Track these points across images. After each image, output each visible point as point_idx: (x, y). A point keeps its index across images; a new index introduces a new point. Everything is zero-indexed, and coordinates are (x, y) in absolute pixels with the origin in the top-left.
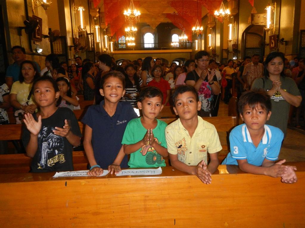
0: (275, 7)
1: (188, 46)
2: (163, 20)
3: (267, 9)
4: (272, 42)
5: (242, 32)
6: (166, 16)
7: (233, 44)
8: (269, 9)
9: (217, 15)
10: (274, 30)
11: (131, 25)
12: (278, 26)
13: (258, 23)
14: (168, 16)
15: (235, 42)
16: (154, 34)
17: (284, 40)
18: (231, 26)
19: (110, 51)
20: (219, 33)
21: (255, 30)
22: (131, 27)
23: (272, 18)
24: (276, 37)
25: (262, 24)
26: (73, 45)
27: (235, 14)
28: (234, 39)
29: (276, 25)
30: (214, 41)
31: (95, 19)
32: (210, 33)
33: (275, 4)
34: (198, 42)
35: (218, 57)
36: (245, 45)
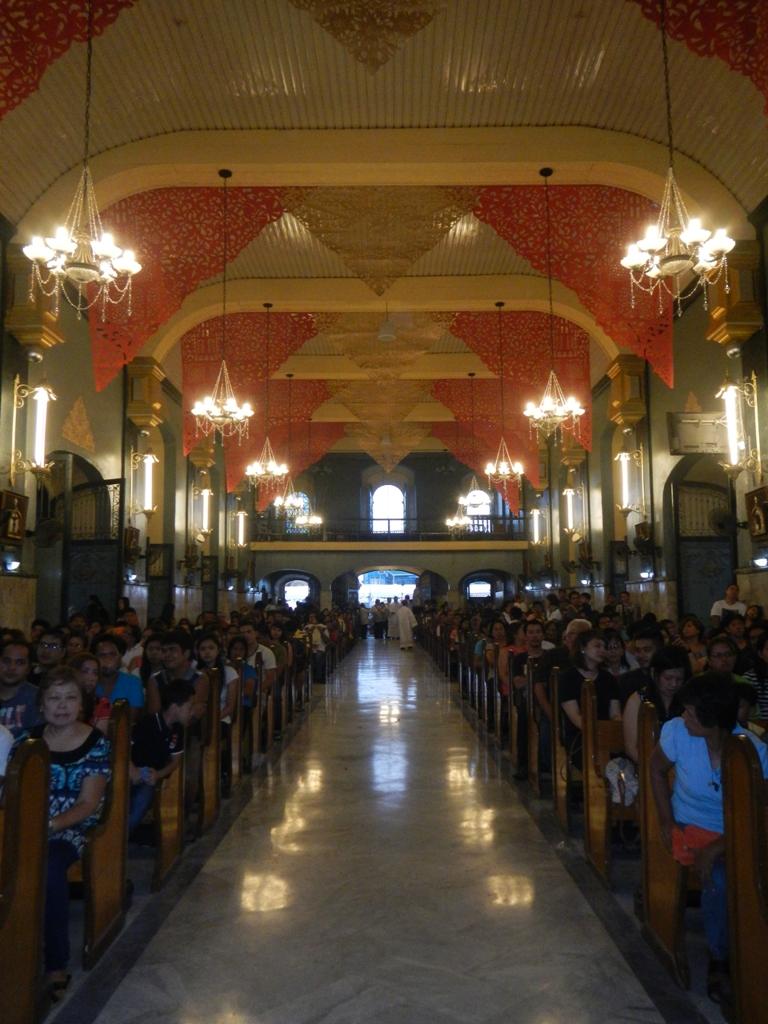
0: (755, 389)
1: (516, 530)
2: (419, 443)
4: (758, 517)
5: (665, 480)
6: (429, 430)
8: (730, 395)
9: (536, 417)
10: (760, 470)
11: (267, 453)
13: (698, 447)
14: (436, 429)
15: (646, 517)
16: (405, 488)
18: (623, 459)
19: (237, 541)
20: (597, 487)
21: (698, 476)
22: (268, 460)
23: (748, 430)
25: (710, 451)
27: (637, 418)
28: (641, 505)
30: (578, 514)
31: (146, 435)
32: (571, 488)
33: (754, 377)
35: (599, 569)
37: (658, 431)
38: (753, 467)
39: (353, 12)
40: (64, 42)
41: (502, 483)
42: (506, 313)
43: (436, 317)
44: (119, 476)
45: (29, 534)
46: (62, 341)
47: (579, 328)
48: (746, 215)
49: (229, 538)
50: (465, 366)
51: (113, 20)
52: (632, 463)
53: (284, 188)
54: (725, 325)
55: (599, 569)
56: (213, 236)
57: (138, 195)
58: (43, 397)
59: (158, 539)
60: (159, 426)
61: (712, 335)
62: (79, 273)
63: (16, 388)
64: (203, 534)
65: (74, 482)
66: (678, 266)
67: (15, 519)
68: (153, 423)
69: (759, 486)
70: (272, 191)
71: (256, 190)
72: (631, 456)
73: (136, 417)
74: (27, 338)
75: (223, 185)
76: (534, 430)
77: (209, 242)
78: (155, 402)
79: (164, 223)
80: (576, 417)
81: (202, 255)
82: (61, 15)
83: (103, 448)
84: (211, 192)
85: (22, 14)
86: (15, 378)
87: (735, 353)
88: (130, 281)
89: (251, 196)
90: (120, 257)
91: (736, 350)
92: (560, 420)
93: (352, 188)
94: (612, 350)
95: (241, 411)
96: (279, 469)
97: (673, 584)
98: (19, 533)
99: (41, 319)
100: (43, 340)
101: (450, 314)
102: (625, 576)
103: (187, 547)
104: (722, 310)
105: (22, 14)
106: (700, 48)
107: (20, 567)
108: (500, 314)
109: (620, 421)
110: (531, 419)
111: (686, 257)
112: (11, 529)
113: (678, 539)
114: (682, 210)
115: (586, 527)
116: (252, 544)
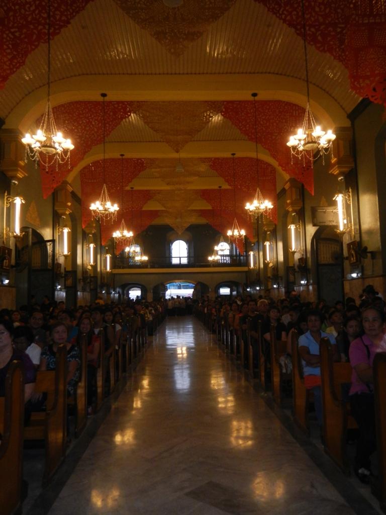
1: (242, 261)
2: (194, 220)
3: (337, 199)
5: (311, 238)
7: (299, 258)
8: (339, 199)
9: (251, 210)
12: (358, 227)
13: (325, 222)
14: (203, 213)
15: (303, 255)
17: (369, 250)
18: (292, 227)
19: (106, 269)
20: (280, 240)
21: (326, 236)
22: (123, 230)
23: (348, 214)
24: (357, 243)
25: (331, 224)
28: (301, 249)
29: (355, 224)
30: (272, 253)
31: (64, 218)
32: (268, 241)
33: (350, 190)
34: (254, 255)
35: (282, 280)
36: (317, 260)
37: (308, 214)
38: (350, 232)
39: (167, 31)
40: (36, 43)
41: (235, 239)
42: (236, 158)
43: (203, 160)
45: (12, 267)
46: (27, 175)
47: (271, 165)
48: (346, 115)
49: (102, 268)
50: (217, 183)
51: (58, 33)
52: (296, 230)
53: (132, 102)
54: (337, 166)
55: (282, 280)
56: (98, 124)
57: (62, 105)
58: (18, 201)
59: (69, 269)
60: (69, 214)
61: (331, 171)
62: (47, 150)
63: (6, 197)
64: (90, 265)
65: (32, 242)
66: (311, 146)
68: (67, 213)
69: (353, 240)
70: (126, 103)
71: (118, 103)
72: (296, 226)
74: (10, 174)
75: (102, 100)
76: (250, 215)
77: (96, 127)
78: (68, 202)
79: (75, 118)
80: (269, 209)
81: (93, 134)
82: (35, 31)
83: (45, 225)
84: (96, 104)
85: (17, 30)
86: (5, 193)
87: (342, 179)
88: (69, 153)
89: (116, 106)
90: (66, 142)
91: (342, 177)
92: (261, 211)
93: (164, 102)
94: (287, 177)
95: (113, 208)
96: (129, 234)
97: (316, 286)
99: (18, 165)
100: (18, 175)
101: (209, 159)
102: (294, 283)
104: (335, 159)
105: (17, 30)
106: (321, 49)
107: (9, 282)
108: (233, 159)
109: (290, 210)
110: (248, 211)
111: (315, 142)
112: (5, 264)
113: (318, 265)
114: (313, 122)
115: (275, 260)
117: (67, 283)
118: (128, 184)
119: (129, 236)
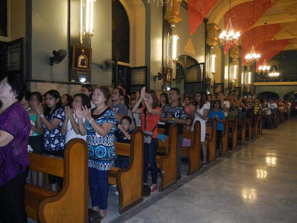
19: (248, 82)
26: (158, 75)
31: (212, 49)
44: (204, 62)
45: (174, 80)
49: (245, 81)
58: (175, 38)
59: (219, 81)
63: (168, 36)
67: (168, 75)
73: (210, 43)
78: (215, 37)
83: (199, 54)
86: (168, 34)
98: (170, 80)
103: (229, 85)
116: (254, 83)
117: (215, 90)
118: (258, 19)
119: (257, 58)
